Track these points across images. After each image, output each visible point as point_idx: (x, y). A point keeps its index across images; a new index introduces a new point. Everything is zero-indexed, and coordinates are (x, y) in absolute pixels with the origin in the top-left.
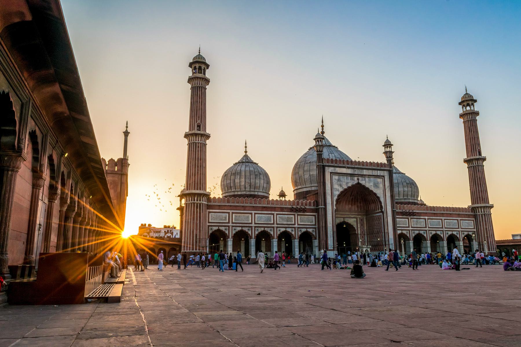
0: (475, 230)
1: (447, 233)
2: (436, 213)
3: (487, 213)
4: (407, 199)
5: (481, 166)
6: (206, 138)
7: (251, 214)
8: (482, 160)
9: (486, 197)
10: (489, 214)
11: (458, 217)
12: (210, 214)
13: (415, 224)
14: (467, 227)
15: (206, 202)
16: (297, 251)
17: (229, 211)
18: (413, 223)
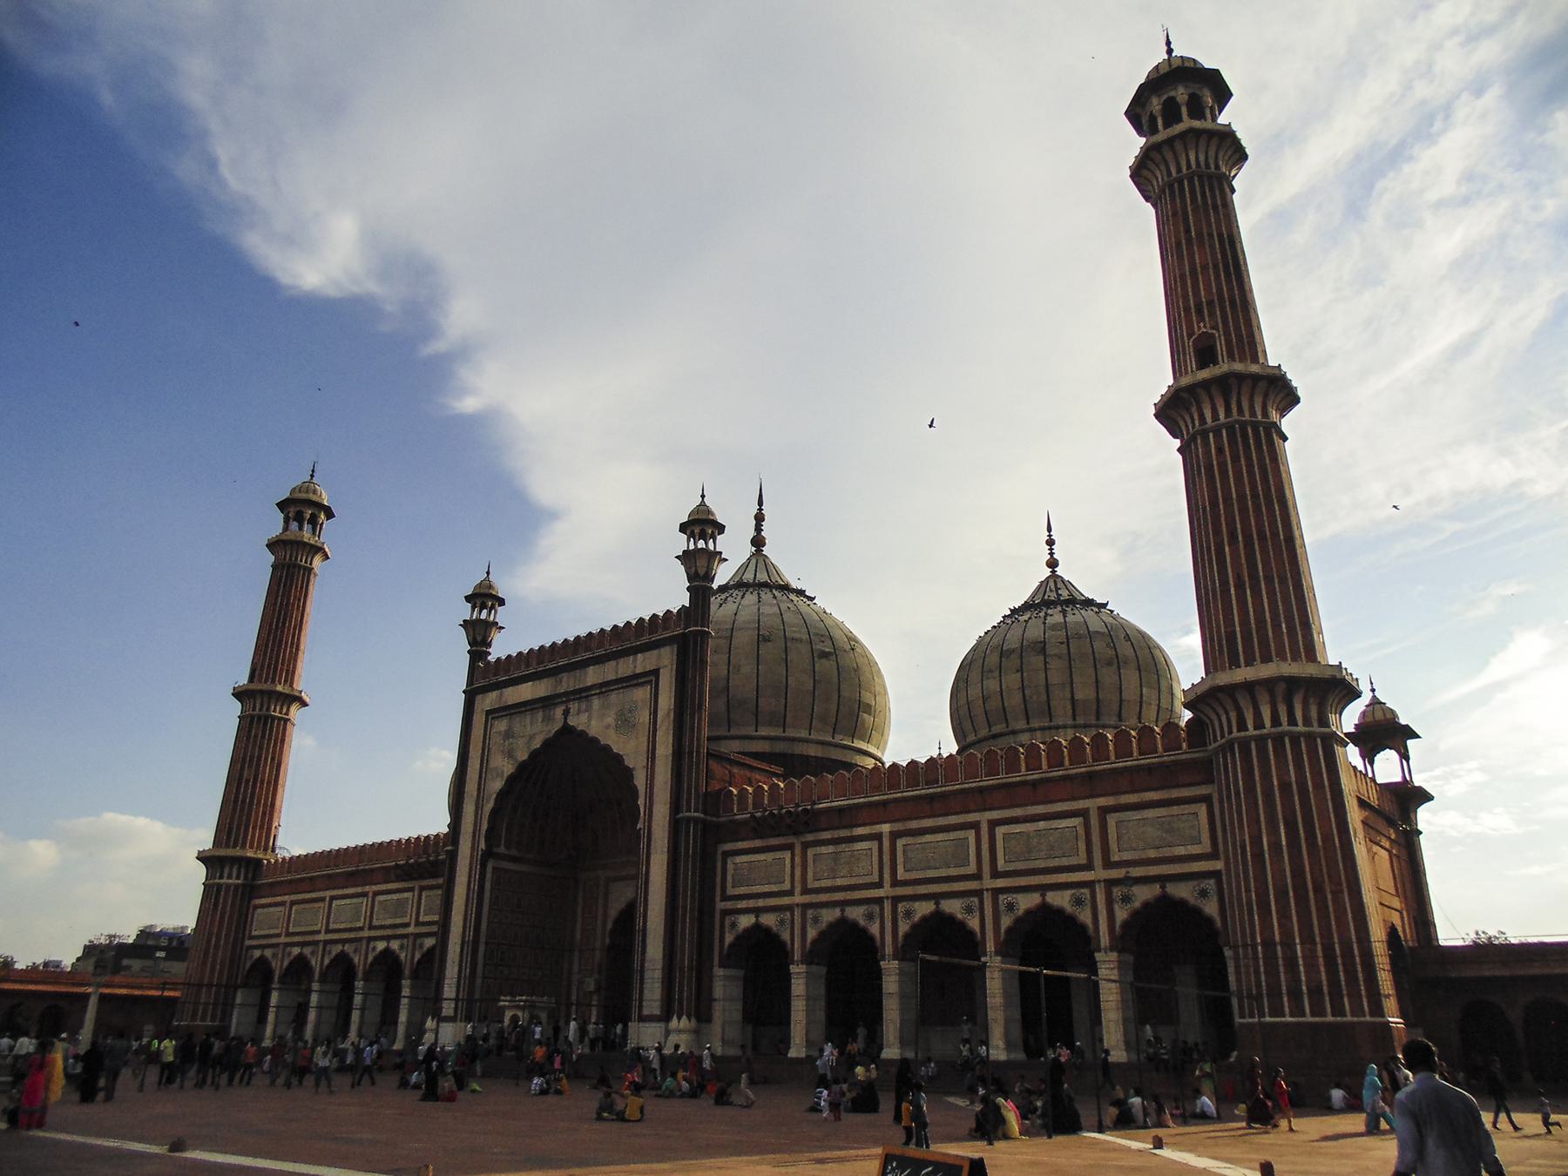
0: (1218, 865)
1: (1011, 907)
2: (943, 795)
3: (1251, 731)
4: (1002, 735)
5: (1211, 435)
6: (265, 699)
7: (322, 899)
8: (1215, 391)
9: (1245, 622)
10: (1261, 740)
11: (1088, 797)
12: (259, 911)
13: (826, 874)
14: (1152, 854)
15: (238, 878)
16: (402, 1023)
17: (286, 898)
18: (815, 867)
